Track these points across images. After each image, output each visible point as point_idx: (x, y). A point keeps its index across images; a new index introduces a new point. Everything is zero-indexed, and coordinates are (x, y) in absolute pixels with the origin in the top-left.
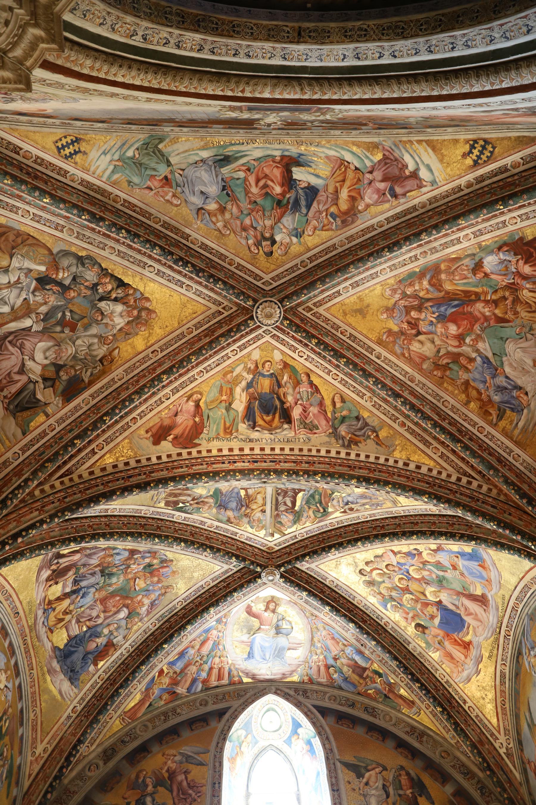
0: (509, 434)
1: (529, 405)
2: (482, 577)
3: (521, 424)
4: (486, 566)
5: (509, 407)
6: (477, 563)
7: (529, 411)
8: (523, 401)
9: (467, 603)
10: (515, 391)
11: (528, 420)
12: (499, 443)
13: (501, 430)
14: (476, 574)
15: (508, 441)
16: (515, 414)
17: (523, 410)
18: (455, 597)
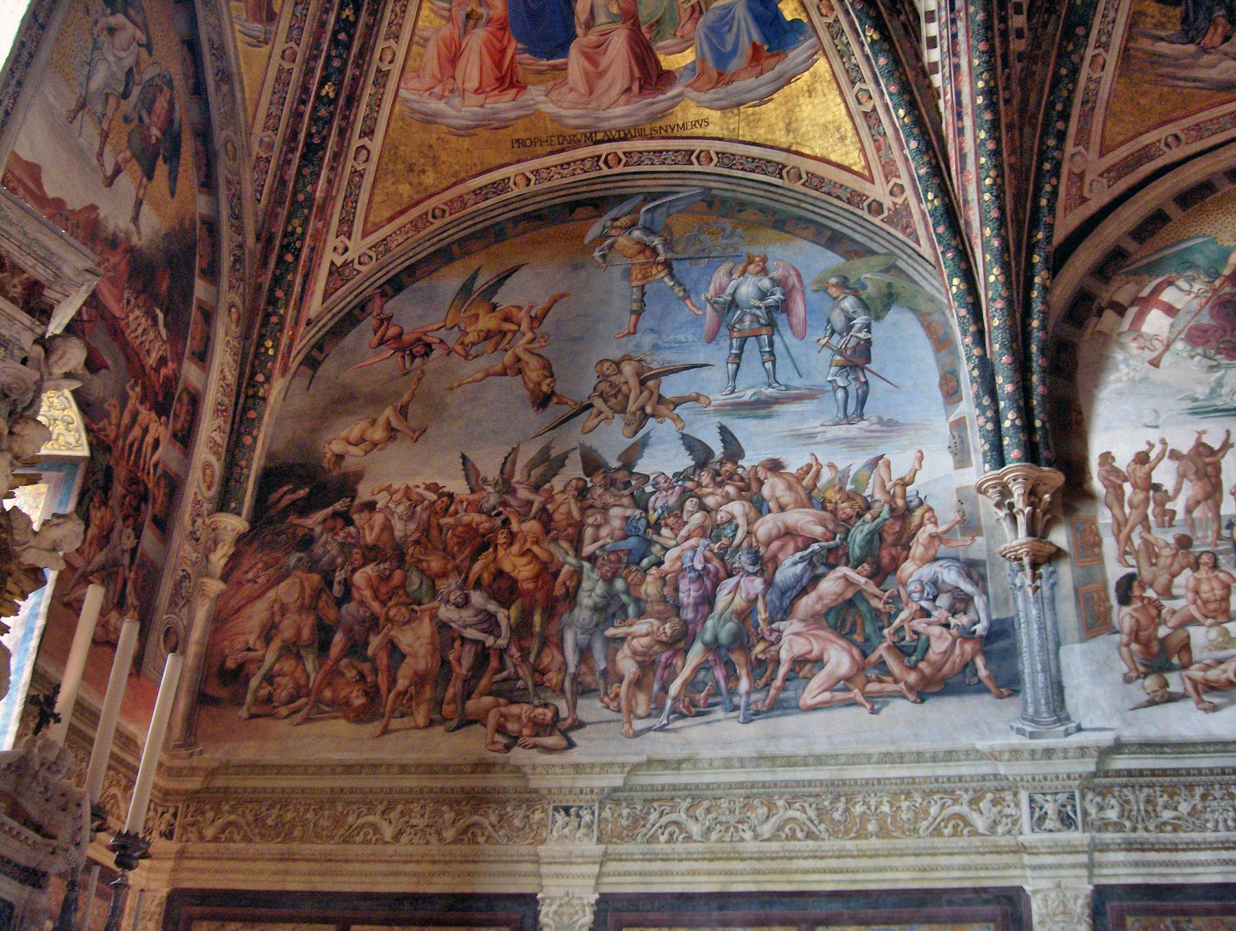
0: (1134, 30)
1: (1205, 51)
2: (722, 59)
3: (1163, 47)
4: (767, 63)
5: (1187, 9)
6: (756, 37)
7: (1194, 56)
8: (1208, 36)
9: (619, 43)
10: (1223, 12)
11: (1176, 59)
12: (1112, 14)
13: (1139, 8)
14: (723, 43)
15: (1120, 32)
16: (1179, 27)
17: (1191, 41)
18: (615, 10)
